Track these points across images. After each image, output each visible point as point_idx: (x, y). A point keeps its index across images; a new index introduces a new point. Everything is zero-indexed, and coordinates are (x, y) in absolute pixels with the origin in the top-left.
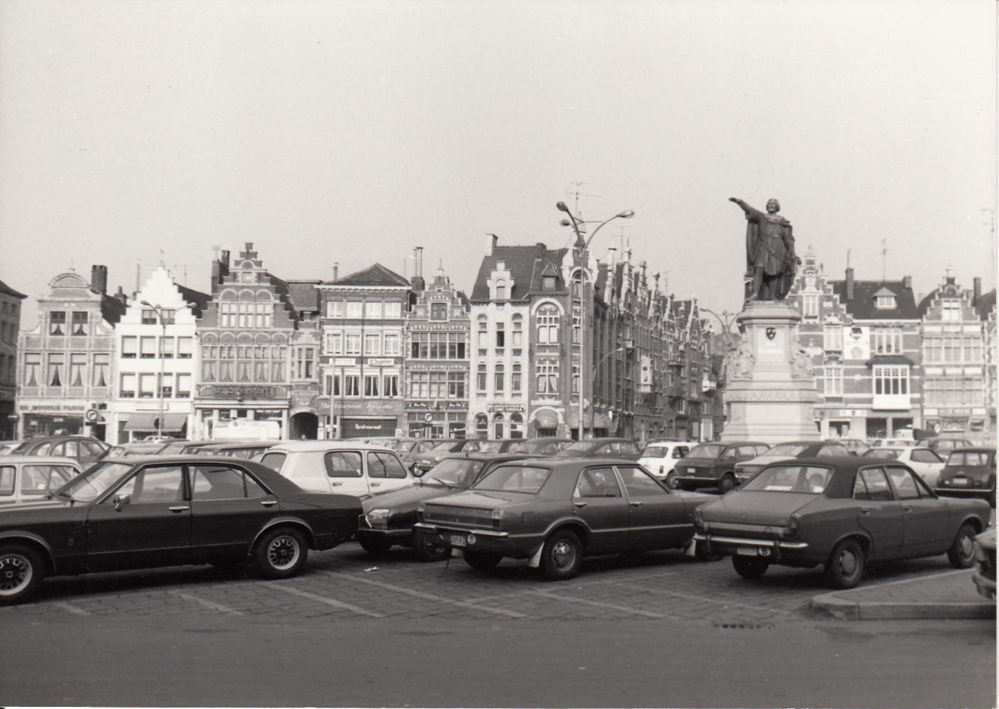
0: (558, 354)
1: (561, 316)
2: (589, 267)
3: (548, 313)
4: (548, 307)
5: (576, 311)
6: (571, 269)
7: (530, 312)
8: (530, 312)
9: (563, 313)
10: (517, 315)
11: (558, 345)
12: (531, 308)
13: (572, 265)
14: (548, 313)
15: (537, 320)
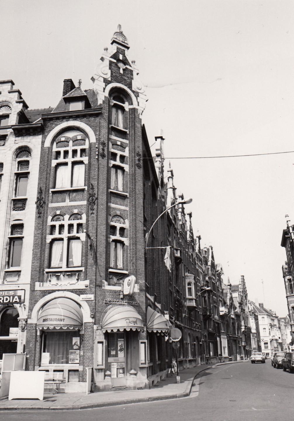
0: (85, 203)
1: (90, 144)
2: (134, 88)
3: (71, 143)
4: (70, 135)
5: (115, 144)
6: (107, 82)
7: (43, 143)
8: (43, 143)
9: (93, 138)
10: (24, 150)
11: (86, 188)
12: (44, 138)
13: (108, 77)
14: (71, 143)
15: (54, 154)
